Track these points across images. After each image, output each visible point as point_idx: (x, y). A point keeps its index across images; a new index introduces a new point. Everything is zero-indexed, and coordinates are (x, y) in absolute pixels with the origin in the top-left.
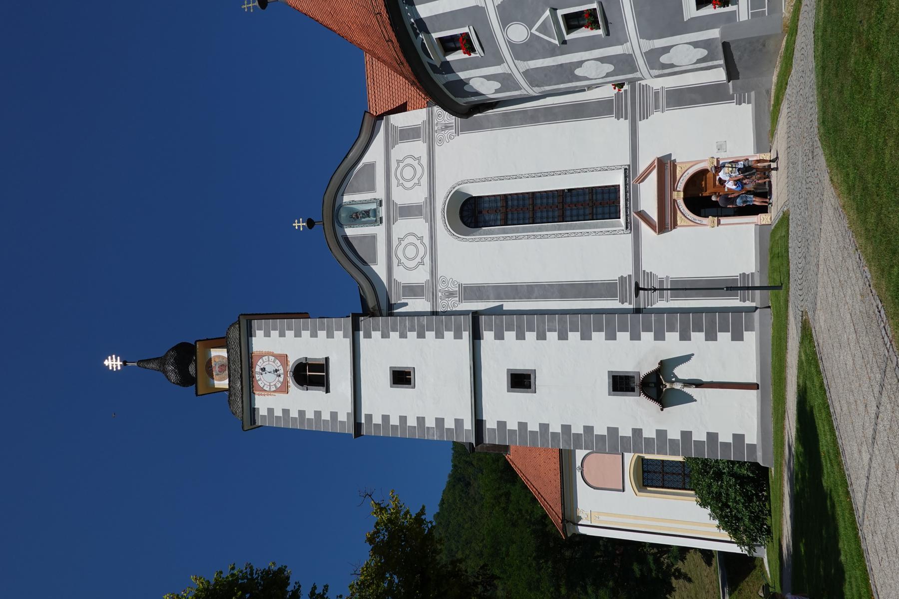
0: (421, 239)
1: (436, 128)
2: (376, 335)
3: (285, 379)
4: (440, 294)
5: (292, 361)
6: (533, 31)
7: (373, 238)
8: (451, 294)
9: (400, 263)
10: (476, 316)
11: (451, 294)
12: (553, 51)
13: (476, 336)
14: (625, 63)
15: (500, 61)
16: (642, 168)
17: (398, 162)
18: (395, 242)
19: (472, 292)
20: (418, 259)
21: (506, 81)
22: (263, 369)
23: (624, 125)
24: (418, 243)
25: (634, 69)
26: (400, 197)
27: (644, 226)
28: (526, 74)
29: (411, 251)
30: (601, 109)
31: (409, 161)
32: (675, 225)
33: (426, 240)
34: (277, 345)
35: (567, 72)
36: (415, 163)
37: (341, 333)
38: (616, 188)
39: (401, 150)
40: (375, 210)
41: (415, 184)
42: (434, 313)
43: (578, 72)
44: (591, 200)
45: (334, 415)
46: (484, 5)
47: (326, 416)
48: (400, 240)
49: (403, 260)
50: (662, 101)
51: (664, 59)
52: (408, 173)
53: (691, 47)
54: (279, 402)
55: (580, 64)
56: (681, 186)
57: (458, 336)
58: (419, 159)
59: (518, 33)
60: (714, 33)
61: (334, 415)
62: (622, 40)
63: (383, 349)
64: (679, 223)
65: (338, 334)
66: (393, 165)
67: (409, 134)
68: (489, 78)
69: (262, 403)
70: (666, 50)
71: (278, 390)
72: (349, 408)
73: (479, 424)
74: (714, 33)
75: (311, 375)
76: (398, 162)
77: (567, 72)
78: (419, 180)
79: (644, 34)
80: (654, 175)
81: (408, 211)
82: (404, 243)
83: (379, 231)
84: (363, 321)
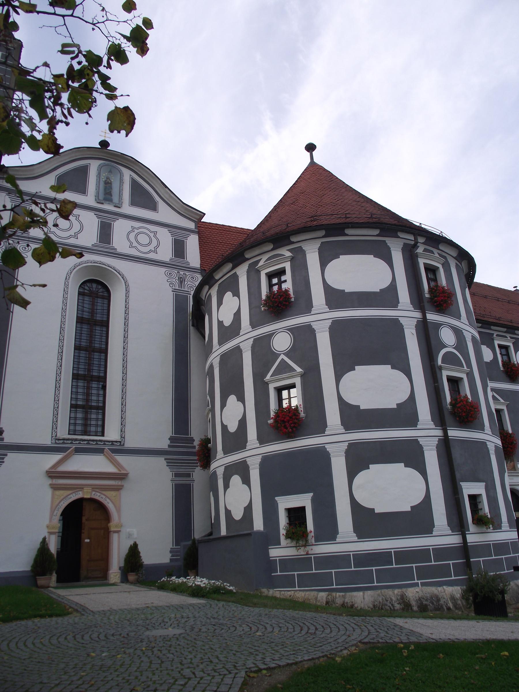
1: (182, 273)
6: (282, 356)
14: (236, 440)
16: (121, 459)
17: (155, 233)
25: (227, 451)
26: (120, 229)
28: (237, 351)
32: (55, 488)
35: (233, 386)
36: (152, 247)
39: (166, 239)
41: (131, 243)
43: (232, 399)
44: (92, 408)
46: (312, 312)
51: (236, 480)
52: (143, 239)
53: (246, 504)
55: (241, 398)
56: (97, 496)
59: (282, 342)
60: (258, 524)
64: (58, 493)
67: (179, 249)
68: (237, 315)
70: (246, 481)
74: (258, 524)
76: (155, 233)
77: (233, 386)
78: (135, 247)
80: (111, 469)
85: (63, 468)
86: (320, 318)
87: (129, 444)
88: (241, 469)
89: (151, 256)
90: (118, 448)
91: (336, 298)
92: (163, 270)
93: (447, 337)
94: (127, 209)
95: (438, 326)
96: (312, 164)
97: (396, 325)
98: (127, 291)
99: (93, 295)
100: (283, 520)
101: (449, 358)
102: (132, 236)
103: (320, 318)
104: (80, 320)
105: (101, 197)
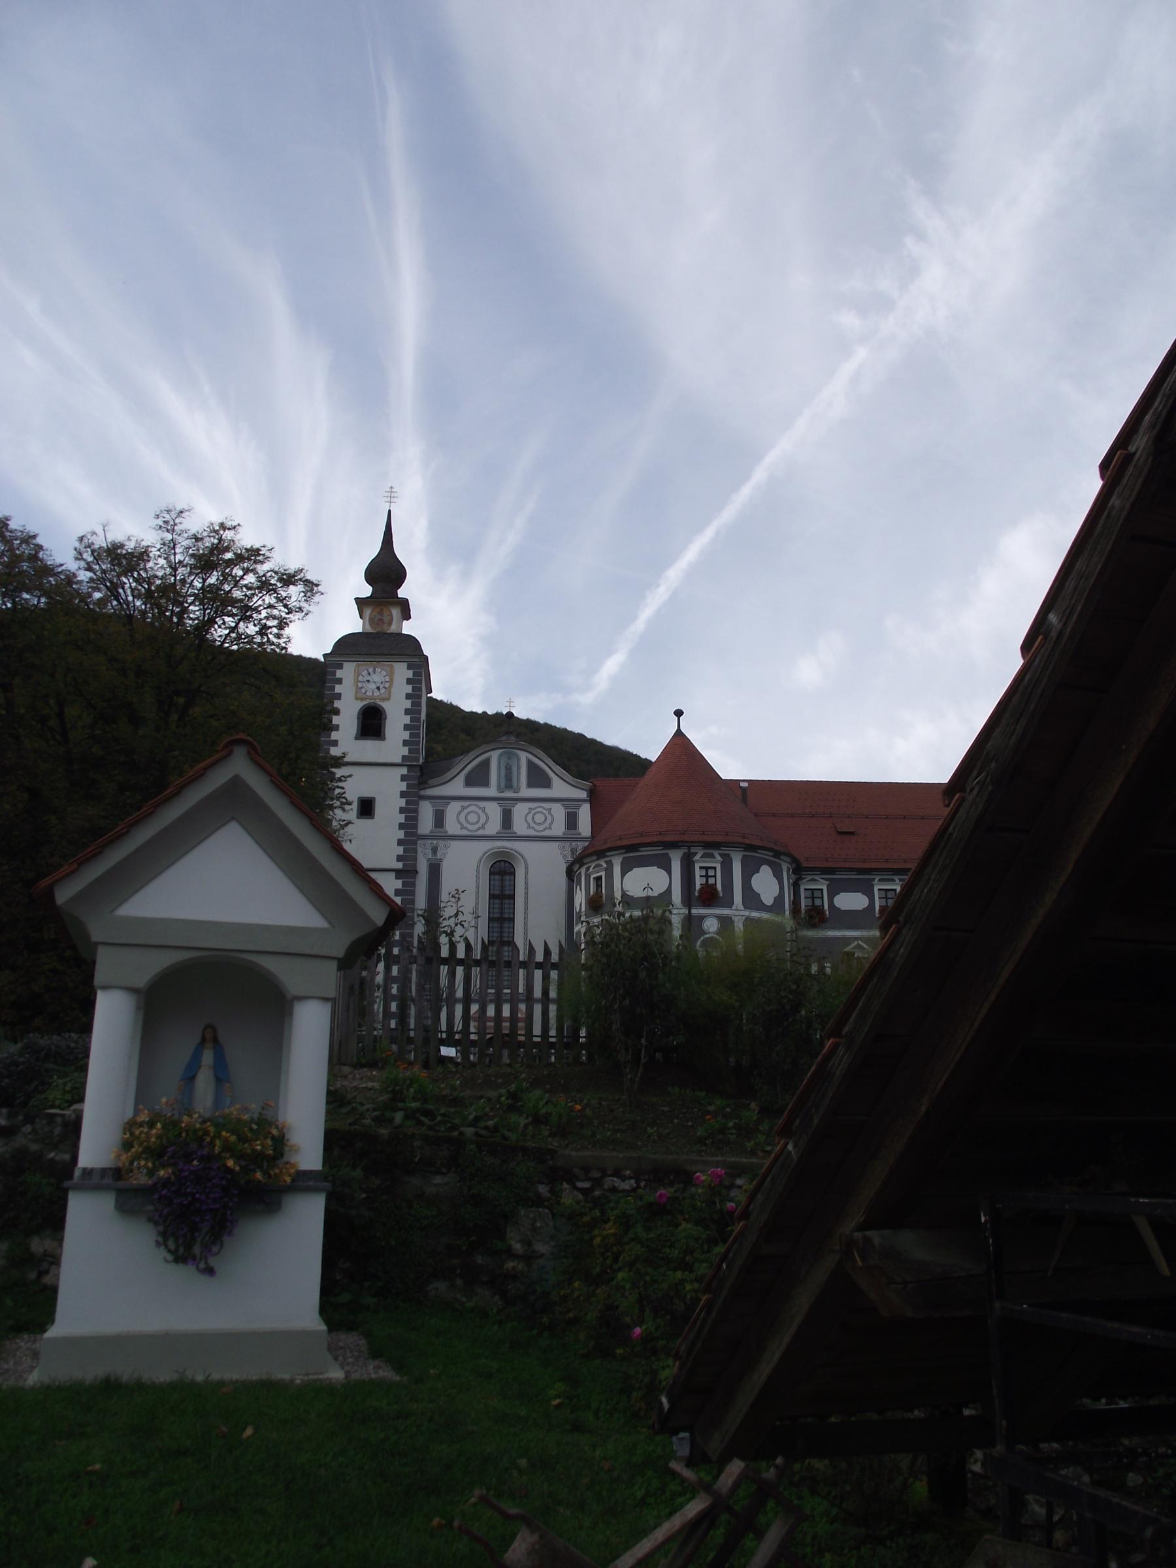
0: (483, 827)
7: (485, 783)
9: (463, 808)
11: (435, 850)
18: (482, 804)
19: (435, 871)
20: (466, 825)
24: (480, 825)
26: (520, 811)
29: (473, 818)
31: (549, 818)
36: (546, 825)
39: (559, 812)
48: (483, 809)
49: (466, 811)
52: (539, 818)
57: (399, 858)
58: (550, 828)
63: (388, 789)
65: (405, 751)
66: (547, 805)
76: (549, 810)
89: (547, 833)
92: (557, 844)
94: (526, 792)
96: (679, 734)
99: (502, 873)
102: (529, 818)
104: (492, 897)
105: (503, 785)
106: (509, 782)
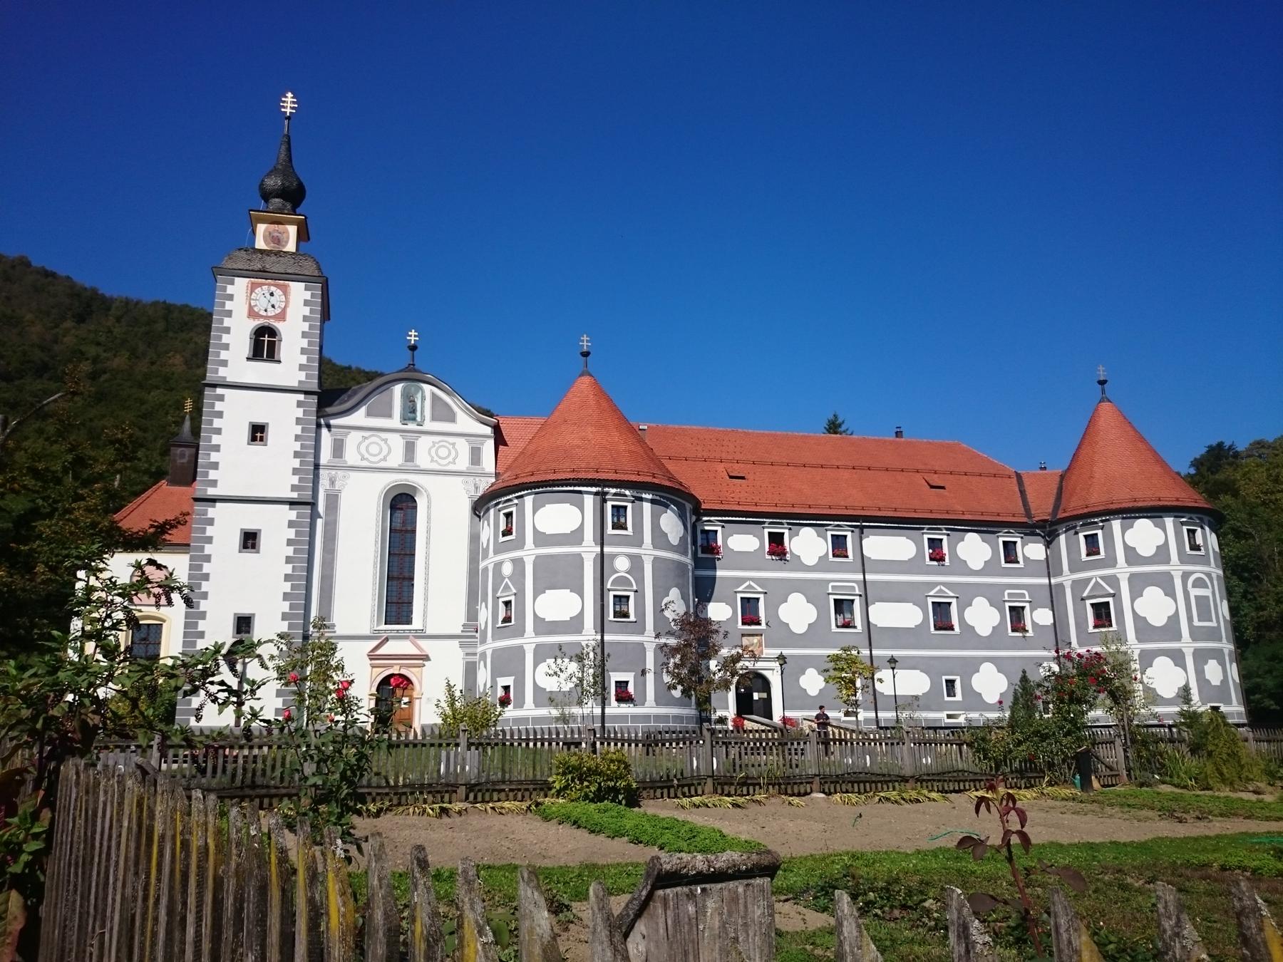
0: (385, 459)
2: (300, 413)
3: (262, 316)
4: (333, 472)
5: (278, 325)
7: (390, 416)
8: (332, 482)
10: (313, 504)
11: (332, 482)
12: (495, 591)
13: (292, 503)
15: (496, 553)
16: (422, 643)
17: (454, 444)
18: (384, 435)
19: (333, 500)
20: (366, 456)
21: (486, 556)
22: (272, 294)
23: (458, 630)
24: (381, 456)
26: (423, 444)
27: (376, 643)
28: (486, 569)
29: (374, 449)
30: (472, 614)
33: (383, 464)
34: (295, 308)
36: (450, 459)
37: (303, 379)
38: (409, 622)
39: (463, 447)
40: (414, 419)
42: (317, 466)
45: (224, 363)
47: (224, 355)
48: (385, 441)
49: (367, 442)
50: (471, 659)
52: (443, 452)
54: (239, 306)
56: (403, 671)
57: (294, 488)
59: (507, 569)
61: (224, 363)
62: (494, 639)
63: (286, 416)
65: (302, 376)
66: (451, 439)
69: (239, 286)
71: (251, 308)
72: (230, 379)
73: (213, 500)
75: (264, 344)
76: (454, 444)
79: (495, 651)
80: (415, 651)
81: (410, 449)
82: (382, 443)
83: (395, 422)
84: (314, 400)
85: (379, 652)
86: (529, 553)
87: (429, 632)
88: (483, 655)
89: (451, 467)
90: (421, 635)
91: (542, 539)
92: (460, 479)
93: (622, 564)
94: (429, 425)
95: (614, 556)
97: (579, 559)
98: (429, 502)
100: (500, 693)
101: (621, 581)
102: (433, 451)
103: (529, 553)
106: (410, 412)
